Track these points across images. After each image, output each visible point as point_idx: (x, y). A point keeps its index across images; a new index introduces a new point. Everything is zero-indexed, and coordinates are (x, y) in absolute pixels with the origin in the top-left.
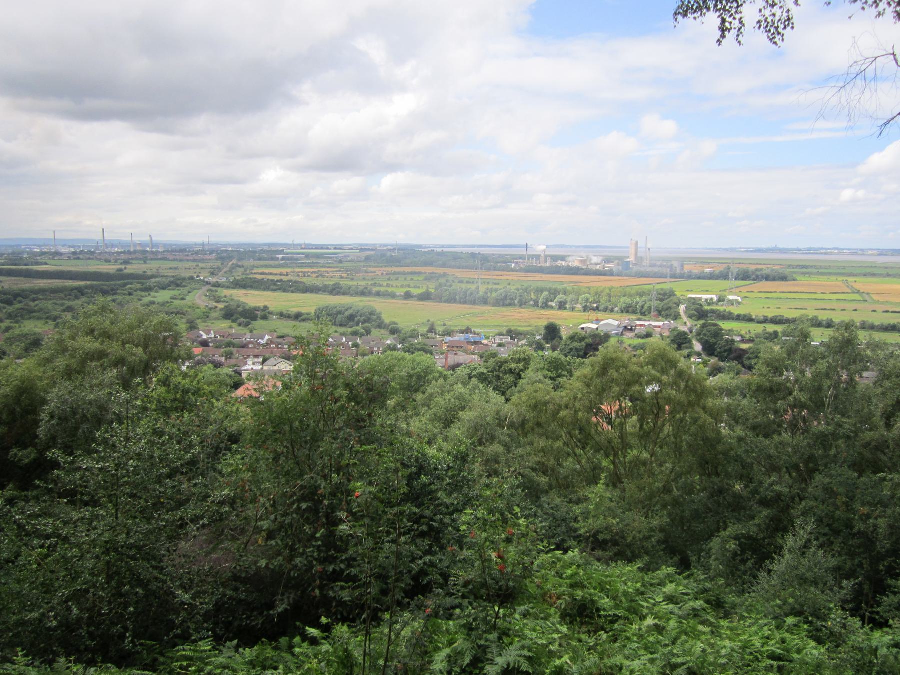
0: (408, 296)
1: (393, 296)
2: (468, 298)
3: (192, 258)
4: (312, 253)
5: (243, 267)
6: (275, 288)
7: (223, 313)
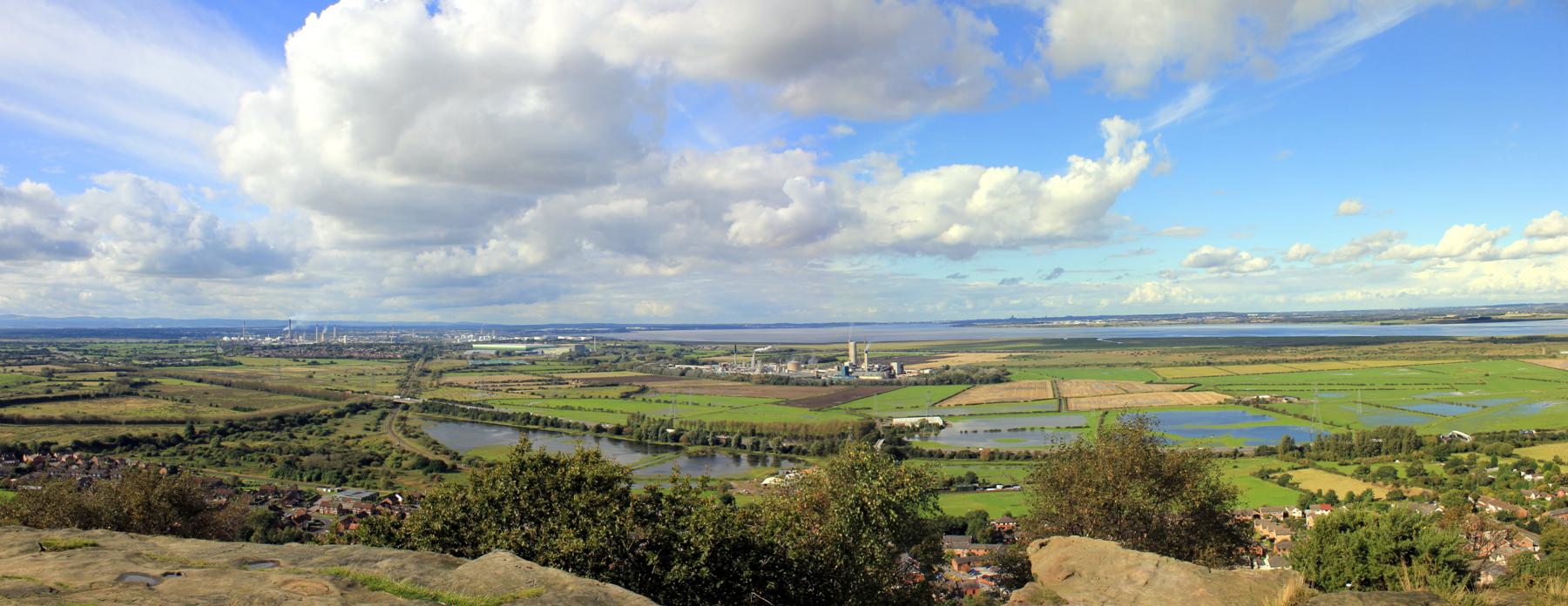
2: (660, 435)
4: (501, 349)
5: (430, 372)
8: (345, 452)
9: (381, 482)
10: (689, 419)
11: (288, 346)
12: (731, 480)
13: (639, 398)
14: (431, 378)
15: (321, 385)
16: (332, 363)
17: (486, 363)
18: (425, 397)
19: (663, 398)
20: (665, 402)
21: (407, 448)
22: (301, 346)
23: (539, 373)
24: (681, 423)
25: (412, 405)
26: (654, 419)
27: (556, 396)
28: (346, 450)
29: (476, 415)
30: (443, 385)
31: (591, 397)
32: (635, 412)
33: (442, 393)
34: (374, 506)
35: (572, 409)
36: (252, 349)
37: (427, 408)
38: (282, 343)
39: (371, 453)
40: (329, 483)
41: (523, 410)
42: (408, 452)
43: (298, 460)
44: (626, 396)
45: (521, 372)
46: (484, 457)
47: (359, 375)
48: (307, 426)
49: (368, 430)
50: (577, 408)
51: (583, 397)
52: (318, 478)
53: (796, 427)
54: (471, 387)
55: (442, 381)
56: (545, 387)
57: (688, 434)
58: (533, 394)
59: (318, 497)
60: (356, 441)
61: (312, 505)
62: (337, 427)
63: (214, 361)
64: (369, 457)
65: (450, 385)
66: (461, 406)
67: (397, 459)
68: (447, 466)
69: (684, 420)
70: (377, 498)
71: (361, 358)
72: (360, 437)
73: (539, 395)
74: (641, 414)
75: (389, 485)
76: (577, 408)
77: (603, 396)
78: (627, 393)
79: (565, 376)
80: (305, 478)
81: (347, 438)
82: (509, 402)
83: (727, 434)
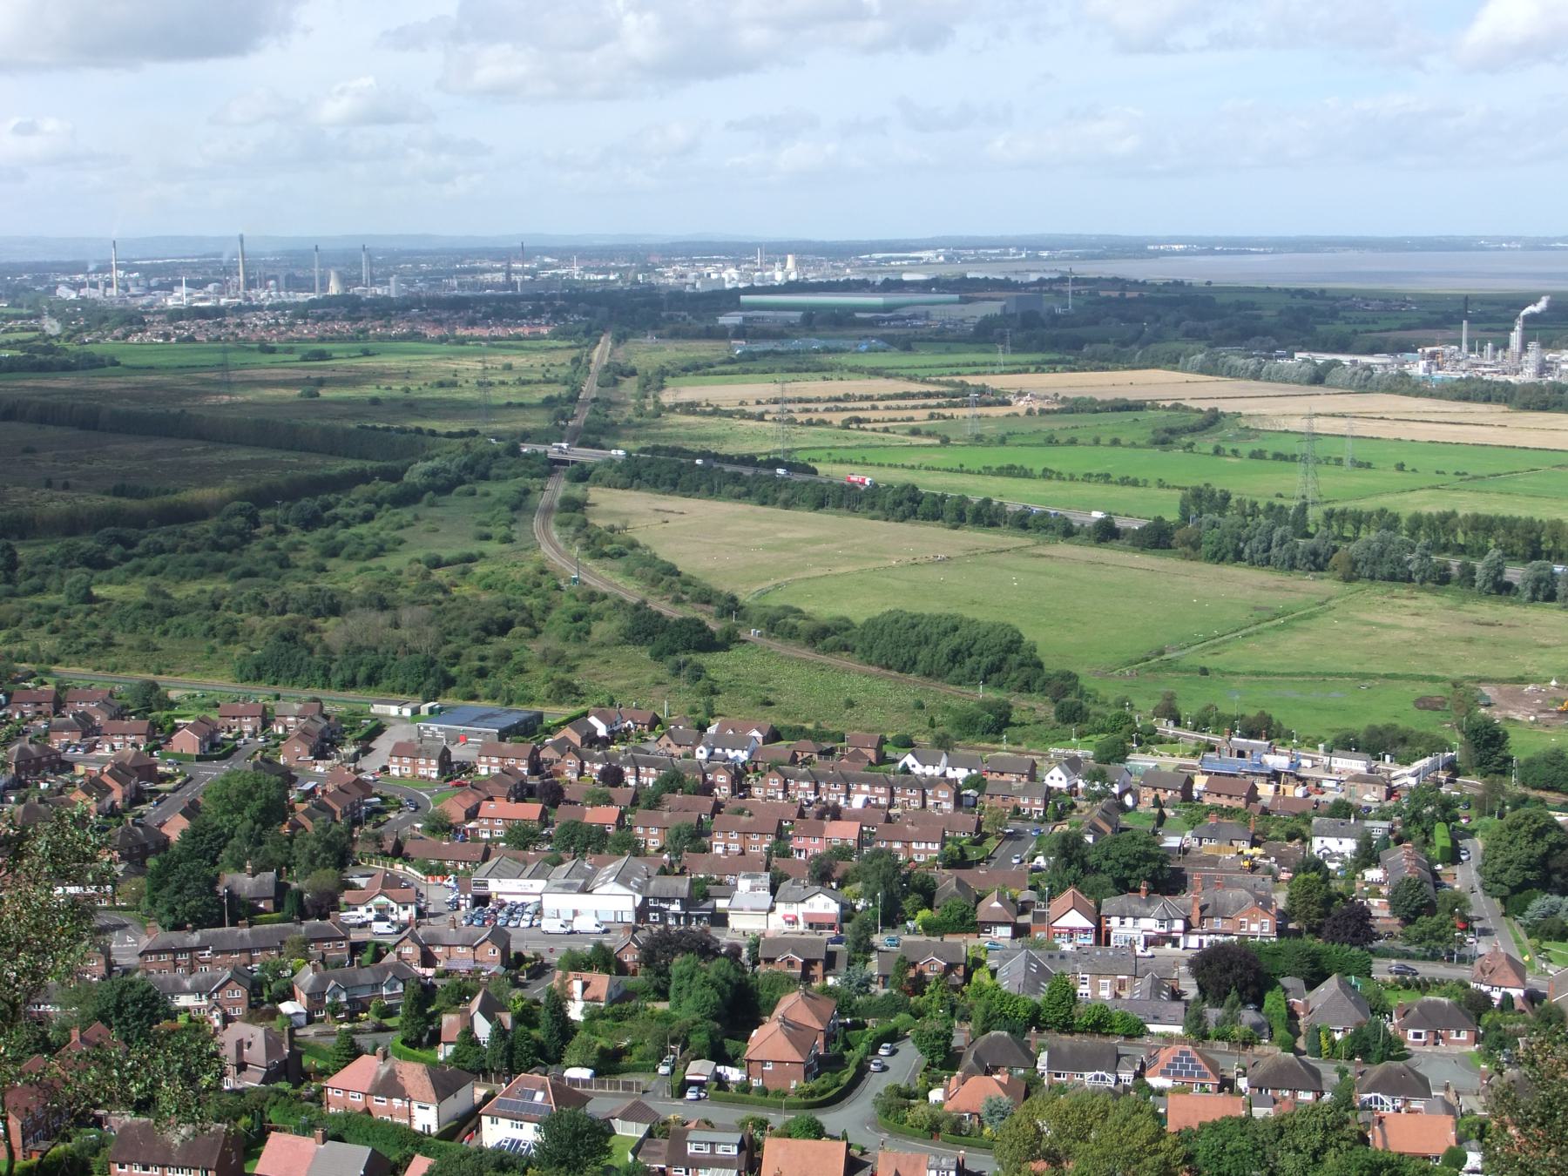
0: (1107, 533)
1: (1069, 532)
2: (1274, 551)
5: (633, 373)
6: (737, 489)
7: (628, 624)
8: (440, 603)
9: (539, 680)
10: (1351, 506)
11: (239, 309)
12: (1481, 680)
13: (1206, 443)
14: (635, 390)
15: (345, 416)
19: (1270, 447)
20: (1278, 456)
21: (601, 587)
22: (272, 308)
24: (1330, 515)
25: (597, 464)
26: (1254, 505)
27: (979, 438)
28: (439, 596)
29: (770, 491)
31: (1073, 442)
32: (1200, 483)
34: (535, 752)
35: (1026, 474)
36: (142, 322)
37: (638, 475)
38: (223, 301)
39: (507, 605)
40: (403, 692)
41: (899, 477)
42: (605, 597)
43: (312, 629)
44: (1165, 439)
46: (807, 608)
47: (441, 385)
48: (321, 533)
49: (487, 537)
50: (1038, 470)
51: (1051, 441)
52: (372, 681)
54: (751, 416)
55: (667, 398)
56: (947, 412)
57: (1353, 546)
58: (915, 432)
59: (378, 730)
60: (459, 567)
61: (367, 751)
62: (399, 534)
63: (39, 357)
64: (502, 613)
65: (690, 408)
67: (578, 617)
68: (713, 634)
69: (1338, 507)
70: (539, 727)
72: (470, 559)
73: (929, 434)
75: (566, 691)
76: (1038, 470)
77: (1105, 440)
78: (1172, 431)
79: (995, 382)
80: (337, 679)
81: (437, 563)
82: (856, 455)
83: (1462, 550)
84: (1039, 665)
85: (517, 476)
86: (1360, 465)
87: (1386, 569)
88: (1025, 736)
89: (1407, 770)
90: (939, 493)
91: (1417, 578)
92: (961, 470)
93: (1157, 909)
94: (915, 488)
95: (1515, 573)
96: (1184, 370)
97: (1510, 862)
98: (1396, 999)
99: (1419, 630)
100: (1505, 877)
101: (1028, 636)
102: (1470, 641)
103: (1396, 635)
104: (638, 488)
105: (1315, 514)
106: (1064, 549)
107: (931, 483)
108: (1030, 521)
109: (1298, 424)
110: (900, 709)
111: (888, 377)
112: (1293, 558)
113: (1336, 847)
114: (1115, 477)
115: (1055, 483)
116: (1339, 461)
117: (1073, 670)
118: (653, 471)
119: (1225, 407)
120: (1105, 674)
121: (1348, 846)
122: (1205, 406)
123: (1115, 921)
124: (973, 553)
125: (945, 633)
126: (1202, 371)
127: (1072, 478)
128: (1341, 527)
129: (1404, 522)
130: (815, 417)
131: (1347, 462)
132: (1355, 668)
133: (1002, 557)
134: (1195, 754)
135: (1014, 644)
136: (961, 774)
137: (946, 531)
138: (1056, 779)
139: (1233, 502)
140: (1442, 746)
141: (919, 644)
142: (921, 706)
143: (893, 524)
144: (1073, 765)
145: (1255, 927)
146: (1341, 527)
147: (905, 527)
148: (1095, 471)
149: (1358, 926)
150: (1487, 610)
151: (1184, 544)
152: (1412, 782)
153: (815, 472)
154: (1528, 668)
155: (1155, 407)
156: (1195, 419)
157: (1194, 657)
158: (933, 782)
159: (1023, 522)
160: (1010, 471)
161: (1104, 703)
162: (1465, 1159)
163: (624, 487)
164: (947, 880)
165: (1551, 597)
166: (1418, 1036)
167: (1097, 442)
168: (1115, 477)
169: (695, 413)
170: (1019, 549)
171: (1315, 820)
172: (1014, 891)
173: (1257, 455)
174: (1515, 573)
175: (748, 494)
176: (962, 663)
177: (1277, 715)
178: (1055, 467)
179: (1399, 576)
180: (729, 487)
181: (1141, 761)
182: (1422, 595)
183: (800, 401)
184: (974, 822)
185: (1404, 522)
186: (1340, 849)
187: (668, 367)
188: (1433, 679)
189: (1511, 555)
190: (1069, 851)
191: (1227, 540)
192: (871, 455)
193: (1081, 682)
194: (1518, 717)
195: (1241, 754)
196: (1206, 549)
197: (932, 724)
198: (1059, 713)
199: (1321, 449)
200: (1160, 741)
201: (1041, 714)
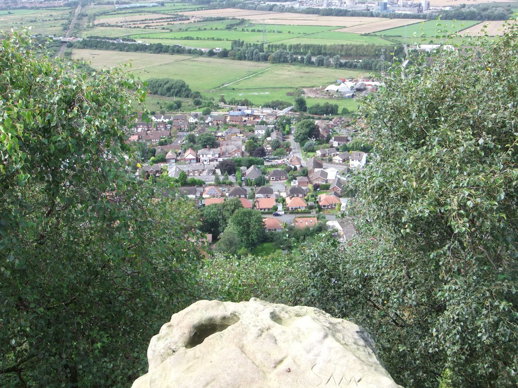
0: (211, 54)
1: (201, 54)
2: (254, 56)
3: (45, 6)
5: (87, 15)
10: (274, 43)
12: (303, 87)
13: (240, 28)
14: (87, 21)
16: (10, 13)
17: (127, 6)
18: (84, 35)
19: (256, 28)
20: (259, 31)
23: (166, 12)
24: (269, 46)
26: (250, 44)
27: (180, 29)
30: (97, 25)
31: (205, 29)
32: (237, 39)
33: (98, 32)
35: (192, 39)
37: (86, 45)
41: (156, 42)
44: (229, 28)
45: (154, 12)
47: (32, 21)
50: (195, 38)
51: (199, 30)
53: (350, 47)
55: (96, 23)
56: (172, 23)
57: (273, 54)
58: (163, 29)
65: (102, 25)
66: (111, 41)
69: (271, 44)
71: (32, 8)
73: (167, 29)
74: (241, 40)
76: (195, 38)
77: (214, 28)
82: (147, 36)
83: (301, 54)
84: (190, 90)
85: (52, 47)
86: (279, 32)
87: (282, 59)
88: (185, 109)
89: (281, 111)
90: (168, 45)
91: (290, 61)
92: (175, 39)
93: (212, 152)
94: (161, 44)
95: (314, 59)
96: (236, 8)
97: (301, 133)
98: (271, 170)
99: (289, 75)
100: (300, 137)
101: (187, 82)
102: (302, 77)
103: (283, 76)
104: (86, 48)
105: (266, 46)
106: (201, 59)
107: (165, 43)
108: (191, 52)
109: (262, 22)
110: (153, 104)
111: (157, 13)
112: (259, 58)
113: (260, 132)
114: (215, 39)
115: (200, 41)
116: (274, 31)
117: (199, 91)
118: (90, 43)
119: (246, 18)
120: (208, 91)
121: (264, 132)
122: (241, 18)
123: (201, 156)
124: (177, 61)
125: (166, 84)
126: (241, 8)
127: (204, 39)
128: (272, 49)
129: (288, 47)
130: (136, 26)
131: (276, 31)
132: (272, 86)
133: (184, 62)
134: (228, 111)
135: (183, 85)
136: (167, 120)
137: (170, 56)
138: (192, 120)
139: (245, 43)
140: (289, 105)
141: (159, 87)
142: (158, 103)
143: (156, 55)
144: (196, 116)
145: (236, 155)
146: (272, 49)
147: (159, 55)
148: (210, 37)
149: (262, 153)
150: (307, 69)
151: (231, 56)
152: (282, 114)
153: (135, 41)
154: (315, 84)
155: (228, 19)
156: (238, 21)
157: (231, 85)
158: (159, 123)
159: (190, 52)
160: (187, 38)
161: (207, 100)
162: (277, 208)
163: (83, 48)
164: (159, 150)
165: (323, 65)
166: (273, 179)
167: (212, 29)
168: (215, 39)
169: (103, 26)
170: (189, 59)
171: (256, 126)
172: (177, 150)
173: (253, 31)
174: (314, 59)
175: (117, 48)
176: (170, 91)
177: (250, 100)
178: (200, 36)
179: (285, 61)
180: (111, 47)
181: (214, 113)
182: (292, 66)
183: (133, 21)
184: (169, 133)
185: (288, 47)
186: (262, 133)
187: (97, 13)
188: (291, 88)
189: (313, 54)
190: (192, 139)
191: (242, 54)
192: (151, 36)
193: (201, 94)
194: (311, 96)
195: (240, 110)
196: (237, 57)
197: (161, 108)
198: (194, 102)
199: (268, 28)
200: (221, 108)
201: (190, 103)
